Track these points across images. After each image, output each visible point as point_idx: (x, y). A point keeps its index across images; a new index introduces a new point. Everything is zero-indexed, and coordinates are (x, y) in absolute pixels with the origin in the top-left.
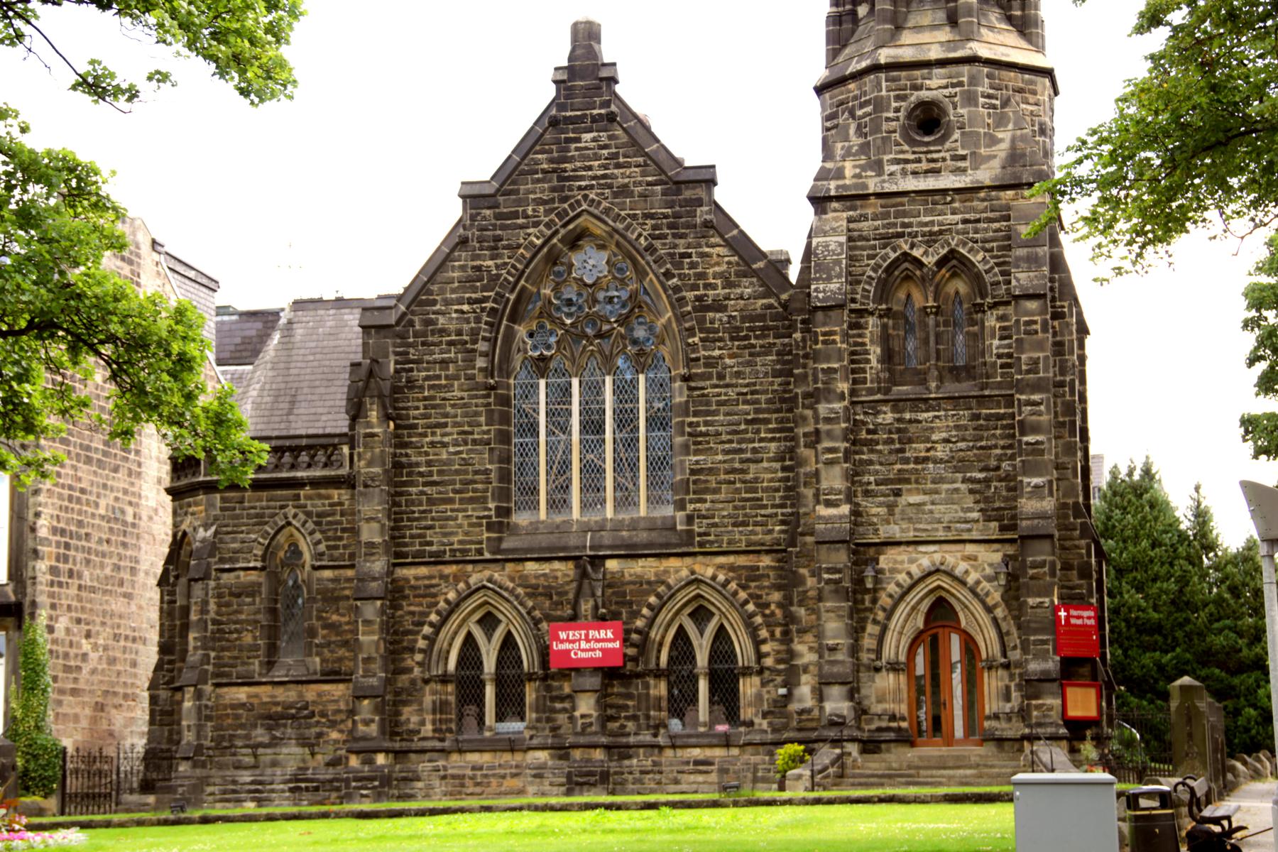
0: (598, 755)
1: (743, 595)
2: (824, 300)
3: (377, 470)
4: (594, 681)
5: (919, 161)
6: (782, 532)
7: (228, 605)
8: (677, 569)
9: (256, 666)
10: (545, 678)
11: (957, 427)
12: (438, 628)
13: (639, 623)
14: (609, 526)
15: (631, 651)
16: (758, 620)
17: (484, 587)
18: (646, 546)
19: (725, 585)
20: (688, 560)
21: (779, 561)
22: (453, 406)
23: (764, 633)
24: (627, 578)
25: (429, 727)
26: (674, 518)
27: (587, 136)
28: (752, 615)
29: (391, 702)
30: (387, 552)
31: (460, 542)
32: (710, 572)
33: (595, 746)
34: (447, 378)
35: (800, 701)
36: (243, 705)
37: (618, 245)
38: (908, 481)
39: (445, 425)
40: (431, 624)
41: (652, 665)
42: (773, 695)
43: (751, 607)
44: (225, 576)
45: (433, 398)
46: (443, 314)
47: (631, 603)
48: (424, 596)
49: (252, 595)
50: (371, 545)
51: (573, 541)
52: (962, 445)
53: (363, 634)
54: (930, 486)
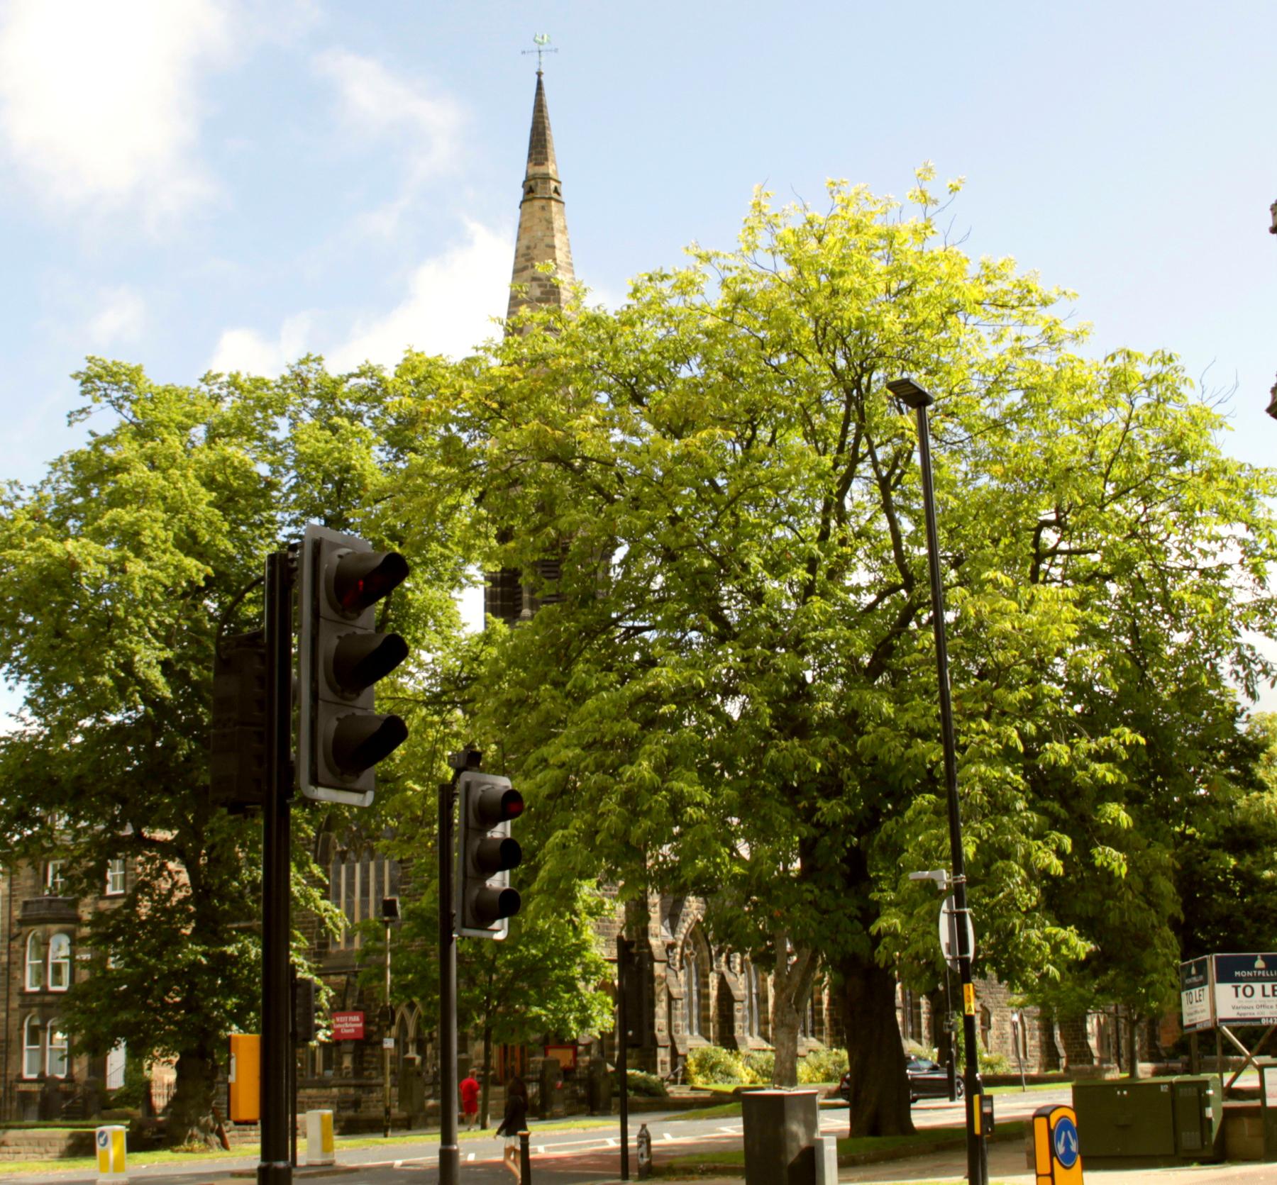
0: (352, 1091)
33: (349, 1086)
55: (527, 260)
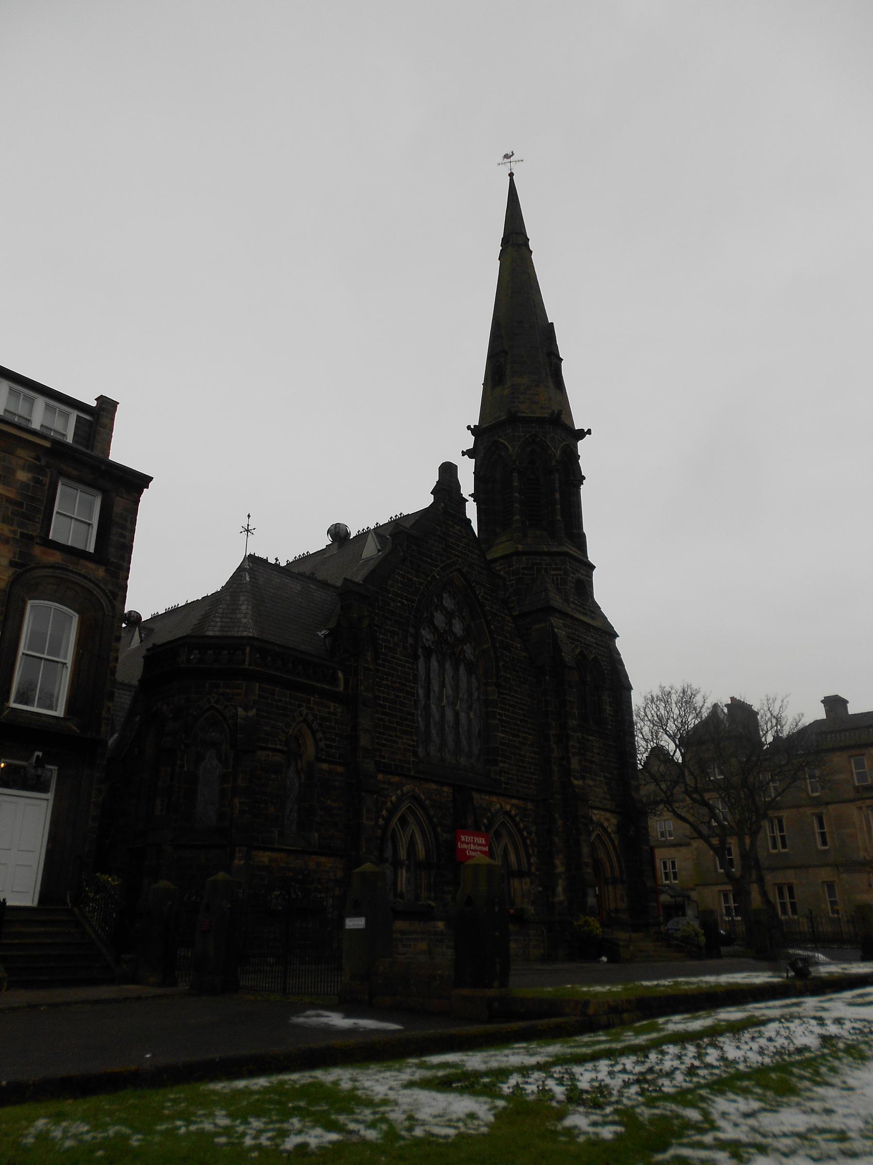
43: (525, 833)
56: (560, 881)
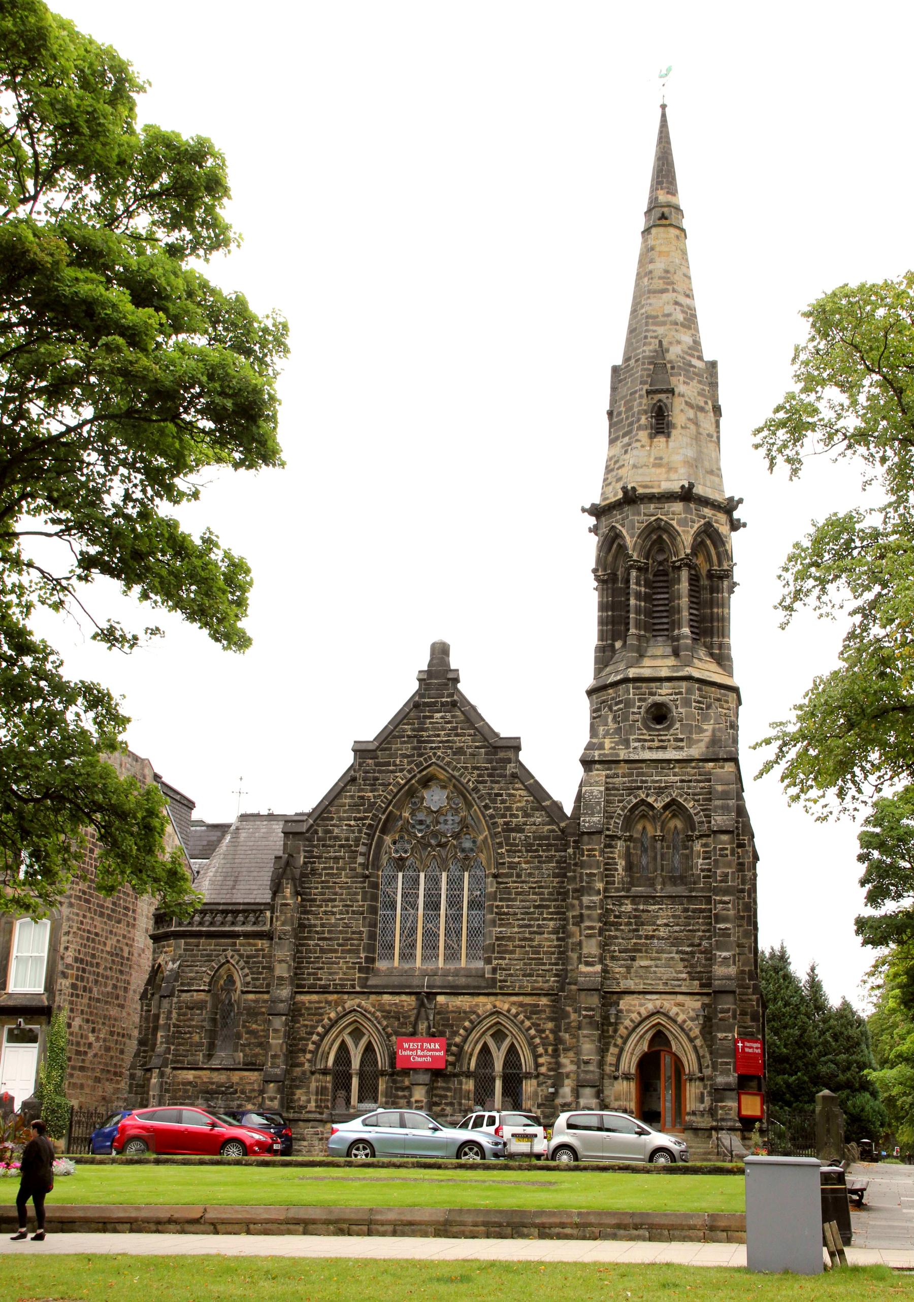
1: (527, 1023)
2: (589, 828)
3: (288, 928)
4: (425, 1078)
5: (653, 741)
6: (555, 981)
7: (185, 1014)
8: (485, 1004)
9: (200, 1057)
10: (392, 1075)
11: (674, 916)
12: (322, 1037)
13: (458, 1039)
14: (440, 973)
15: (451, 1059)
16: (537, 1040)
17: (355, 1010)
18: (464, 987)
19: (516, 1016)
20: (492, 998)
21: (553, 1001)
22: (340, 888)
23: (540, 1050)
24: (451, 1008)
25: (313, 1104)
26: (484, 969)
27: (438, 715)
28: (533, 1037)
29: (288, 1086)
30: (292, 984)
31: (340, 979)
32: (506, 1006)
34: (338, 869)
35: (563, 1097)
36: (190, 1083)
37: (454, 786)
38: (640, 951)
39: (335, 900)
40: (318, 1034)
41: (465, 1069)
42: (545, 1093)
43: (532, 1032)
44: (184, 995)
45: (328, 882)
46: (337, 826)
47: (452, 1026)
48: (314, 1015)
49: (201, 1009)
50: (281, 978)
51: (416, 982)
52: (677, 928)
53: (273, 1038)
54: (654, 955)
55: (668, 284)
56: (567, 1082)
